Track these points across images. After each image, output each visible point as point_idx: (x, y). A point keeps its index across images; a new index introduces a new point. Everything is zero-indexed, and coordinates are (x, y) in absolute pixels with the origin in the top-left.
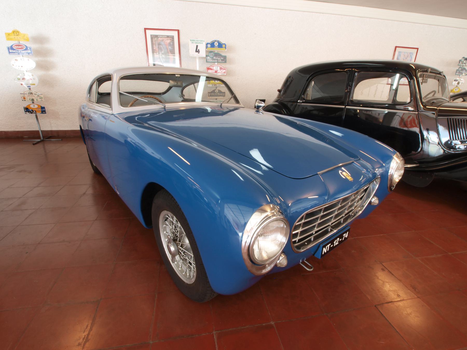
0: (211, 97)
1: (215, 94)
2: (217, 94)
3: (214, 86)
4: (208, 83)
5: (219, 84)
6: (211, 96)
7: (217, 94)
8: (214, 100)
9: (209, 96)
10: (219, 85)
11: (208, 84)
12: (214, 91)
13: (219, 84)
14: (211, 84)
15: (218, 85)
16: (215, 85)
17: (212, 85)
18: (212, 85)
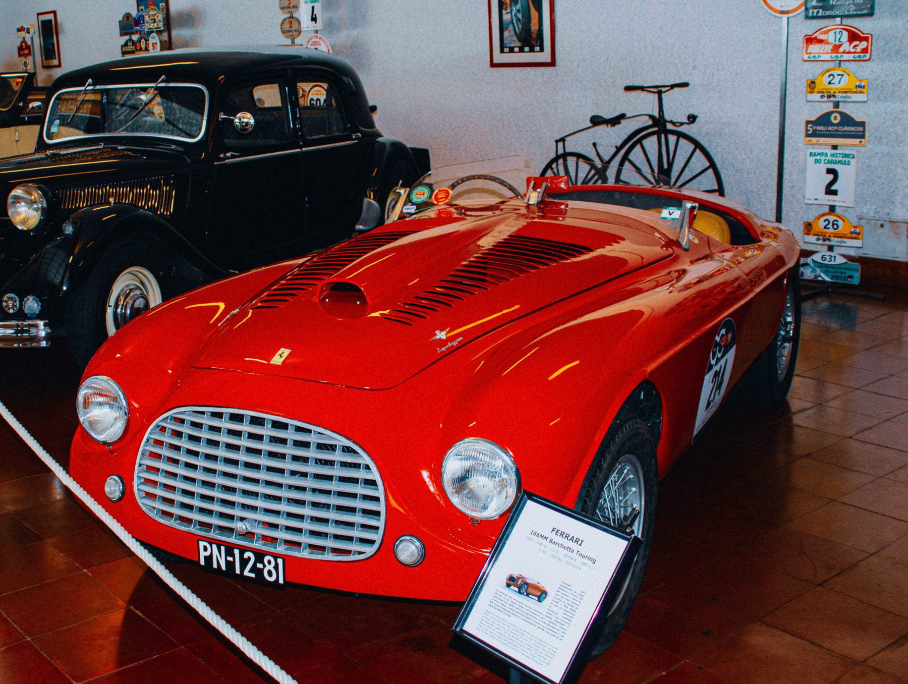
0: (814, 140)
1: (830, 128)
2: (835, 128)
3: (825, 99)
4: (811, 90)
5: (843, 92)
6: (815, 134)
7: (835, 128)
8: (824, 151)
9: (807, 135)
10: (844, 95)
11: (810, 92)
12: (824, 119)
13: (846, 92)
14: (818, 92)
15: (841, 95)
16: (829, 97)
17: (822, 97)
18: (820, 95)
